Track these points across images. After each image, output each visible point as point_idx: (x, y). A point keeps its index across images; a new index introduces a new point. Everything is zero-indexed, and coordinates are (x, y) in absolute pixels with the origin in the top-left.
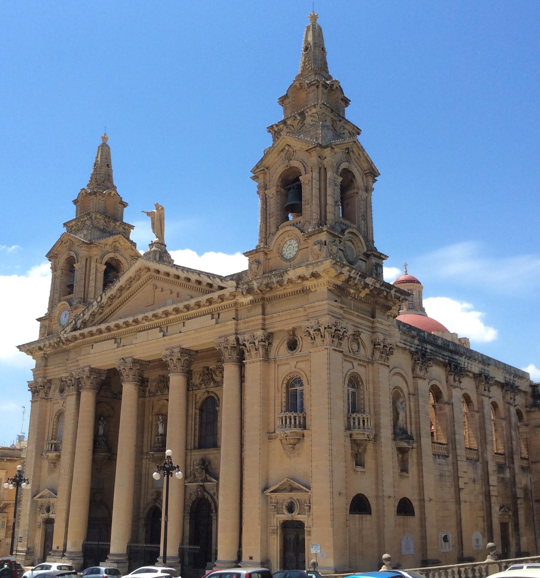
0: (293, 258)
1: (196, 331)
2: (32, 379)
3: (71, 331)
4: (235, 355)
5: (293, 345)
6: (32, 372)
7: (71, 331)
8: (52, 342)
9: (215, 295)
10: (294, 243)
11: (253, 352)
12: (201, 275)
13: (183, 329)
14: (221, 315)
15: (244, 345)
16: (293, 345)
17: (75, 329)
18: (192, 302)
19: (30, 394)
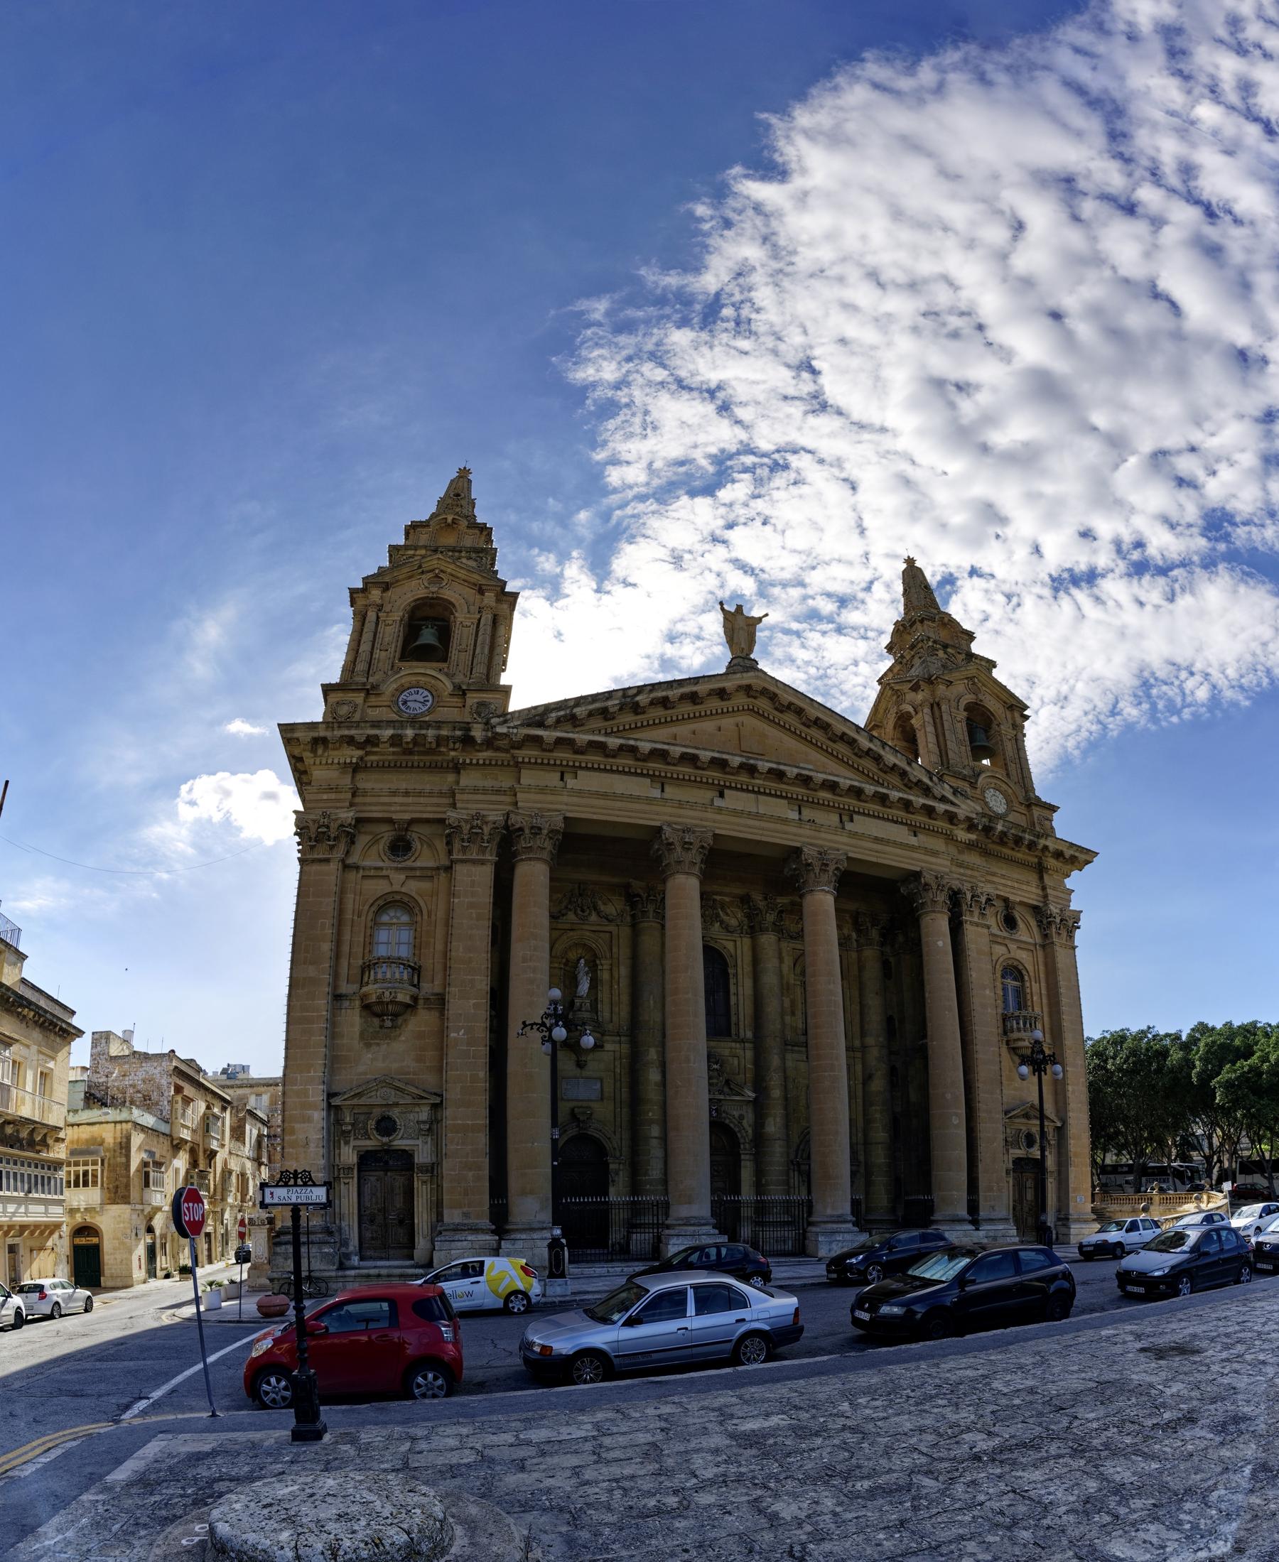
1: (877, 840)
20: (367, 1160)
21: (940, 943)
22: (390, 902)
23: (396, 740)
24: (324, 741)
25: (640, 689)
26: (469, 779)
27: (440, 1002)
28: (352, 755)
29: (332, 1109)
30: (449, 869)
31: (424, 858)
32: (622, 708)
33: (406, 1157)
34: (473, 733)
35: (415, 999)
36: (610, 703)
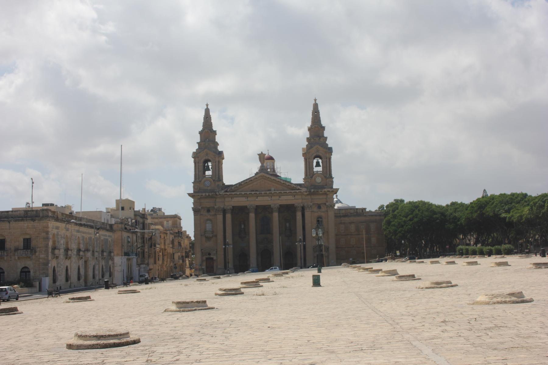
0: (320, 183)
2: (193, 207)
3: (224, 192)
4: (301, 209)
5: (319, 207)
6: (192, 204)
7: (224, 192)
8: (210, 194)
9: (297, 191)
10: (320, 179)
11: (308, 209)
12: (292, 184)
13: (280, 199)
14: (296, 196)
15: (305, 207)
16: (319, 207)
17: (226, 191)
18: (288, 192)
19: (193, 212)
20: (207, 259)
21: (298, 218)
22: (208, 220)
23: (206, 195)
24: (194, 195)
25: (242, 182)
26: (218, 200)
27: (216, 236)
28: (199, 197)
29: (202, 253)
30: (216, 215)
31: (212, 213)
32: (239, 186)
33: (212, 259)
34: (217, 194)
35: (213, 236)
36: (237, 186)
